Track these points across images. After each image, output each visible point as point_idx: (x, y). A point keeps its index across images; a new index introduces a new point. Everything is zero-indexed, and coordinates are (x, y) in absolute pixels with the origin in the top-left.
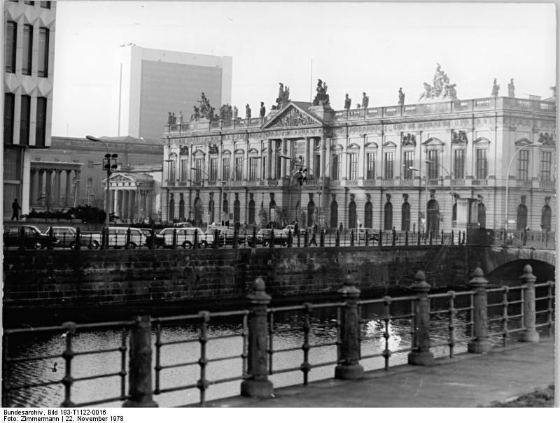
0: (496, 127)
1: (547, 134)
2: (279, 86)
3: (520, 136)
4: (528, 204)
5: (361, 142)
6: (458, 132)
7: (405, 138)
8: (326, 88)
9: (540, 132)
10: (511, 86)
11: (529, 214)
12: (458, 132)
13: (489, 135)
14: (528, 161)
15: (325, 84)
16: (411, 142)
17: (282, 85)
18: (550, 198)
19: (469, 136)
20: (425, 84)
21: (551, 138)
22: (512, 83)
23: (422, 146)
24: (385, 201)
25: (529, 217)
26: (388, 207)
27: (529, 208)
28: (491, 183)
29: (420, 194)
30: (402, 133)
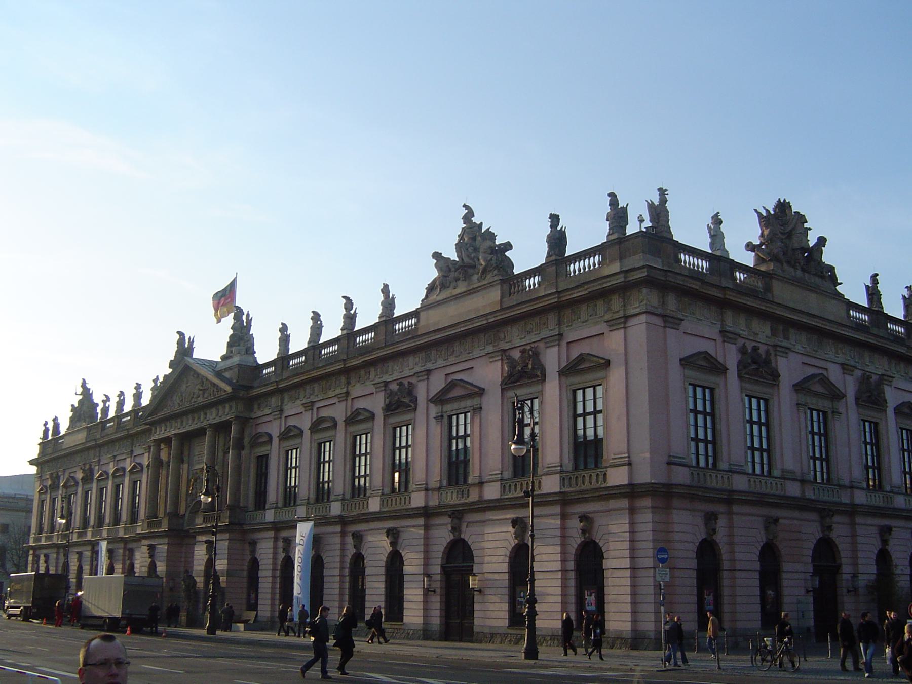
0: (627, 318)
1: (755, 349)
2: (178, 337)
3: (693, 346)
4: (721, 537)
5: (305, 422)
6: (516, 354)
7: (391, 394)
8: (249, 321)
9: (740, 342)
10: (659, 212)
11: (726, 565)
12: (516, 354)
13: (613, 344)
14: (713, 415)
15: (248, 315)
16: (406, 400)
17: (181, 334)
18: (776, 521)
19: (552, 359)
20: (437, 256)
21: (767, 362)
22: (663, 201)
23: (431, 405)
24: (351, 551)
25: (725, 574)
26: (357, 565)
27: (724, 549)
28: (618, 477)
29: (427, 527)
30: (386, 383)
